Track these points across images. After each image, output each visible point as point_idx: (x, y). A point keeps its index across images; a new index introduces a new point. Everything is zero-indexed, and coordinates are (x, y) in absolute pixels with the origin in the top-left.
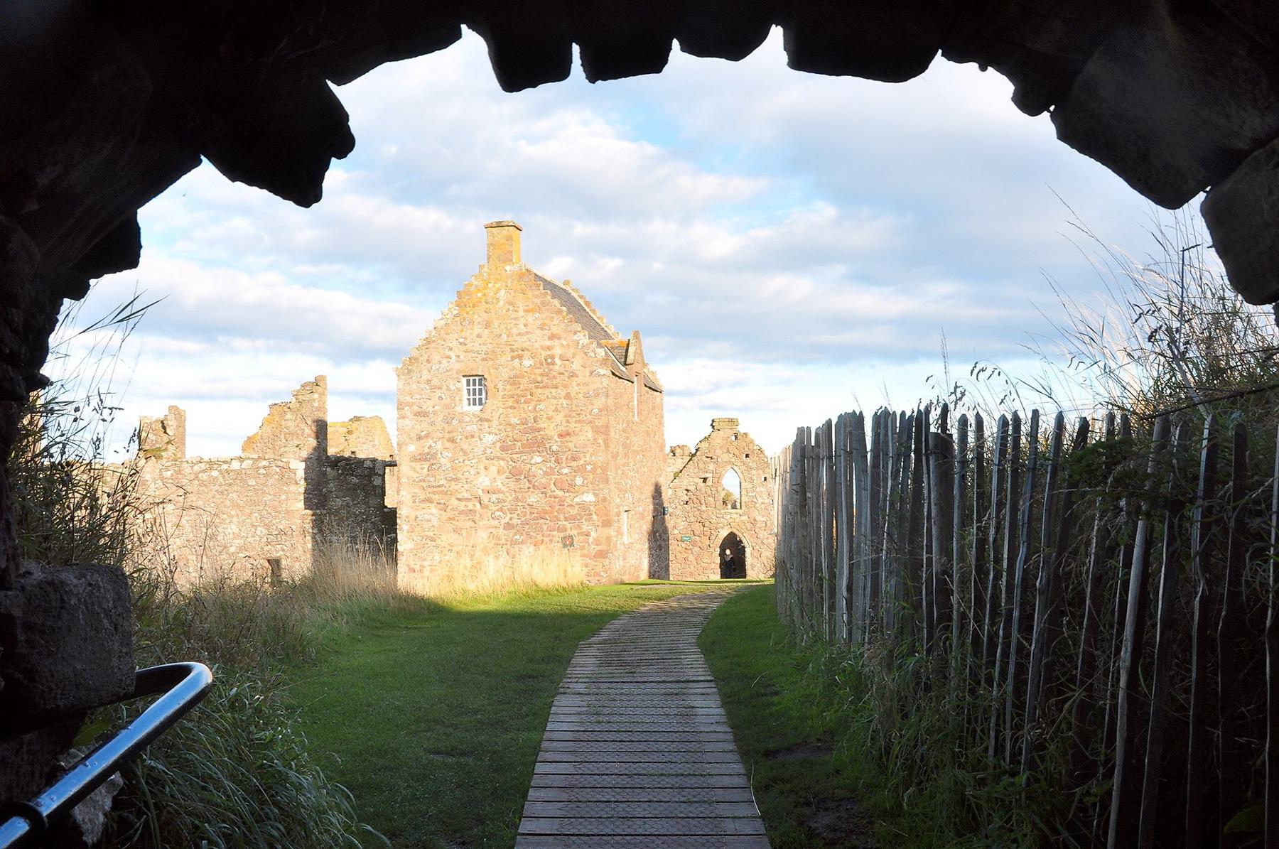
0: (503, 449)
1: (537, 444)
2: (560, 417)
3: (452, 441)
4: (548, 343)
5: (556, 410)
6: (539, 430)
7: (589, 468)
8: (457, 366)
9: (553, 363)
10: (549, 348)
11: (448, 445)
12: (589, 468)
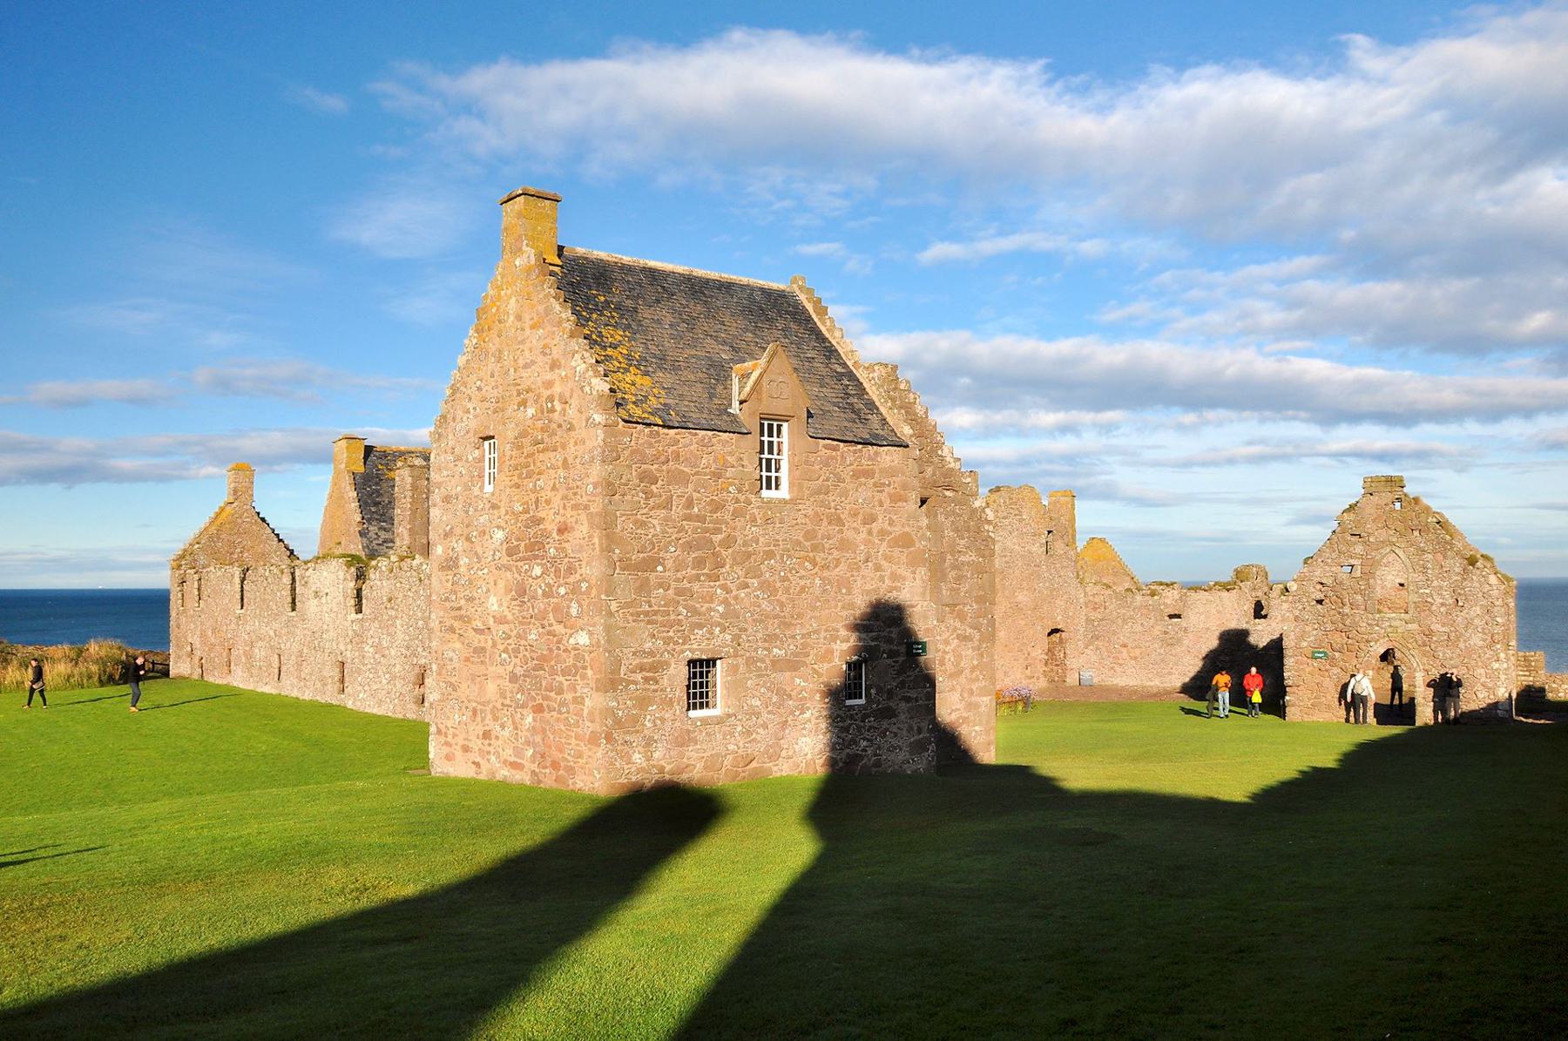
0: (511, 552)
1: (535, 549)
2: (557, 501)
3: (468, 539)
4: (549, 376)
5: (554, 488)
6: (539, 521)
7: (584, 586)
8: (473, 424)
9: (553, 410)
10: (549, 384)
11: (466, 544)
12: (584, 586)
